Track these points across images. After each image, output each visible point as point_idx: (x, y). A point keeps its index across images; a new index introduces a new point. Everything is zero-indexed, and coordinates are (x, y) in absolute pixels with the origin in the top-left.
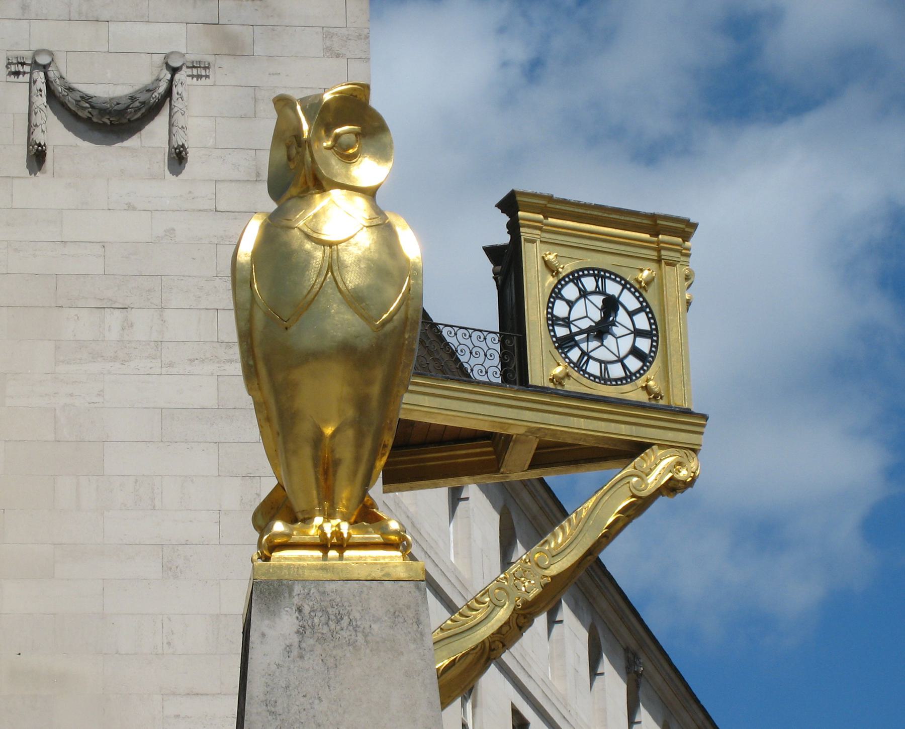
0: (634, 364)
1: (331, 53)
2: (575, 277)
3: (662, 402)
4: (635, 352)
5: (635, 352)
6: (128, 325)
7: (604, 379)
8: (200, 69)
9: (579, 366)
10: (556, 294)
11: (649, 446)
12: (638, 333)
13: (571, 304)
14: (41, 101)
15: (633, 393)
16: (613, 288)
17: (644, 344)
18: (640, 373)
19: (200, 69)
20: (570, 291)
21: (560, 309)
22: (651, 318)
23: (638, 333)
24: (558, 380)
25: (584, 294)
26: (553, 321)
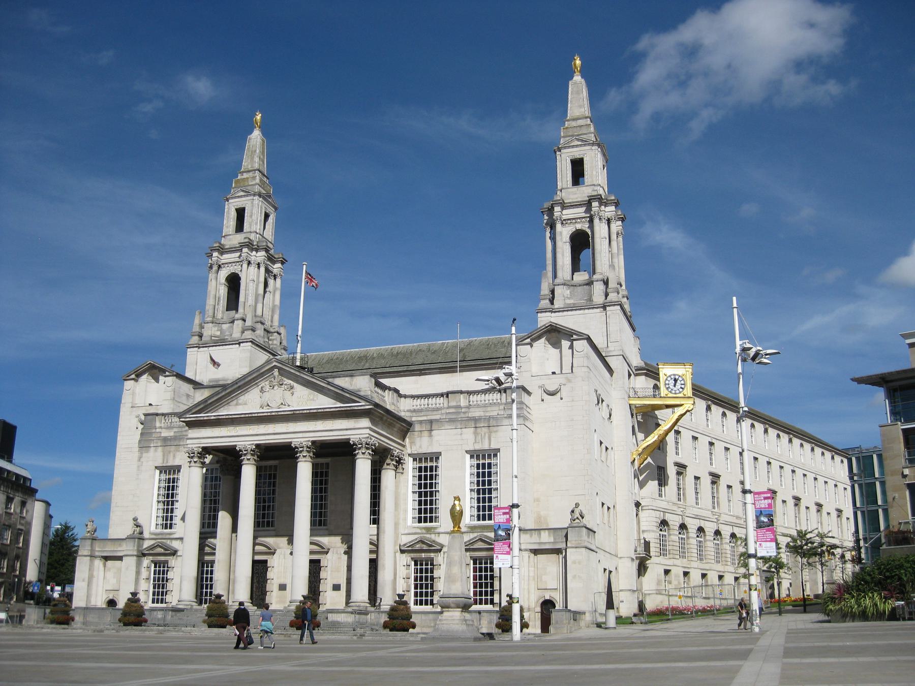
0: (681, 390)
1: (583, 381)
2: (670, 376)
3: (686, 396)
4: (681, 388)
5: (681, 388)
6: (555, 425)
7: (675, 394)
8: (564, 385)
9: (670, 392)
10: (666, 380)
11: (683, 404)
12: (682, 384)
13: (669, 381)
14: (543, 392)
15: (681, 395)
16: (677, 377)
17: (683, 386)
18: (682, 391)
19: (564, 385)
20: (669, 379)
21: (667, 382)
22: (684, 382)
23: (682, 384)
24: (666, 395)
25: (672, 379)
26: (666, 384)
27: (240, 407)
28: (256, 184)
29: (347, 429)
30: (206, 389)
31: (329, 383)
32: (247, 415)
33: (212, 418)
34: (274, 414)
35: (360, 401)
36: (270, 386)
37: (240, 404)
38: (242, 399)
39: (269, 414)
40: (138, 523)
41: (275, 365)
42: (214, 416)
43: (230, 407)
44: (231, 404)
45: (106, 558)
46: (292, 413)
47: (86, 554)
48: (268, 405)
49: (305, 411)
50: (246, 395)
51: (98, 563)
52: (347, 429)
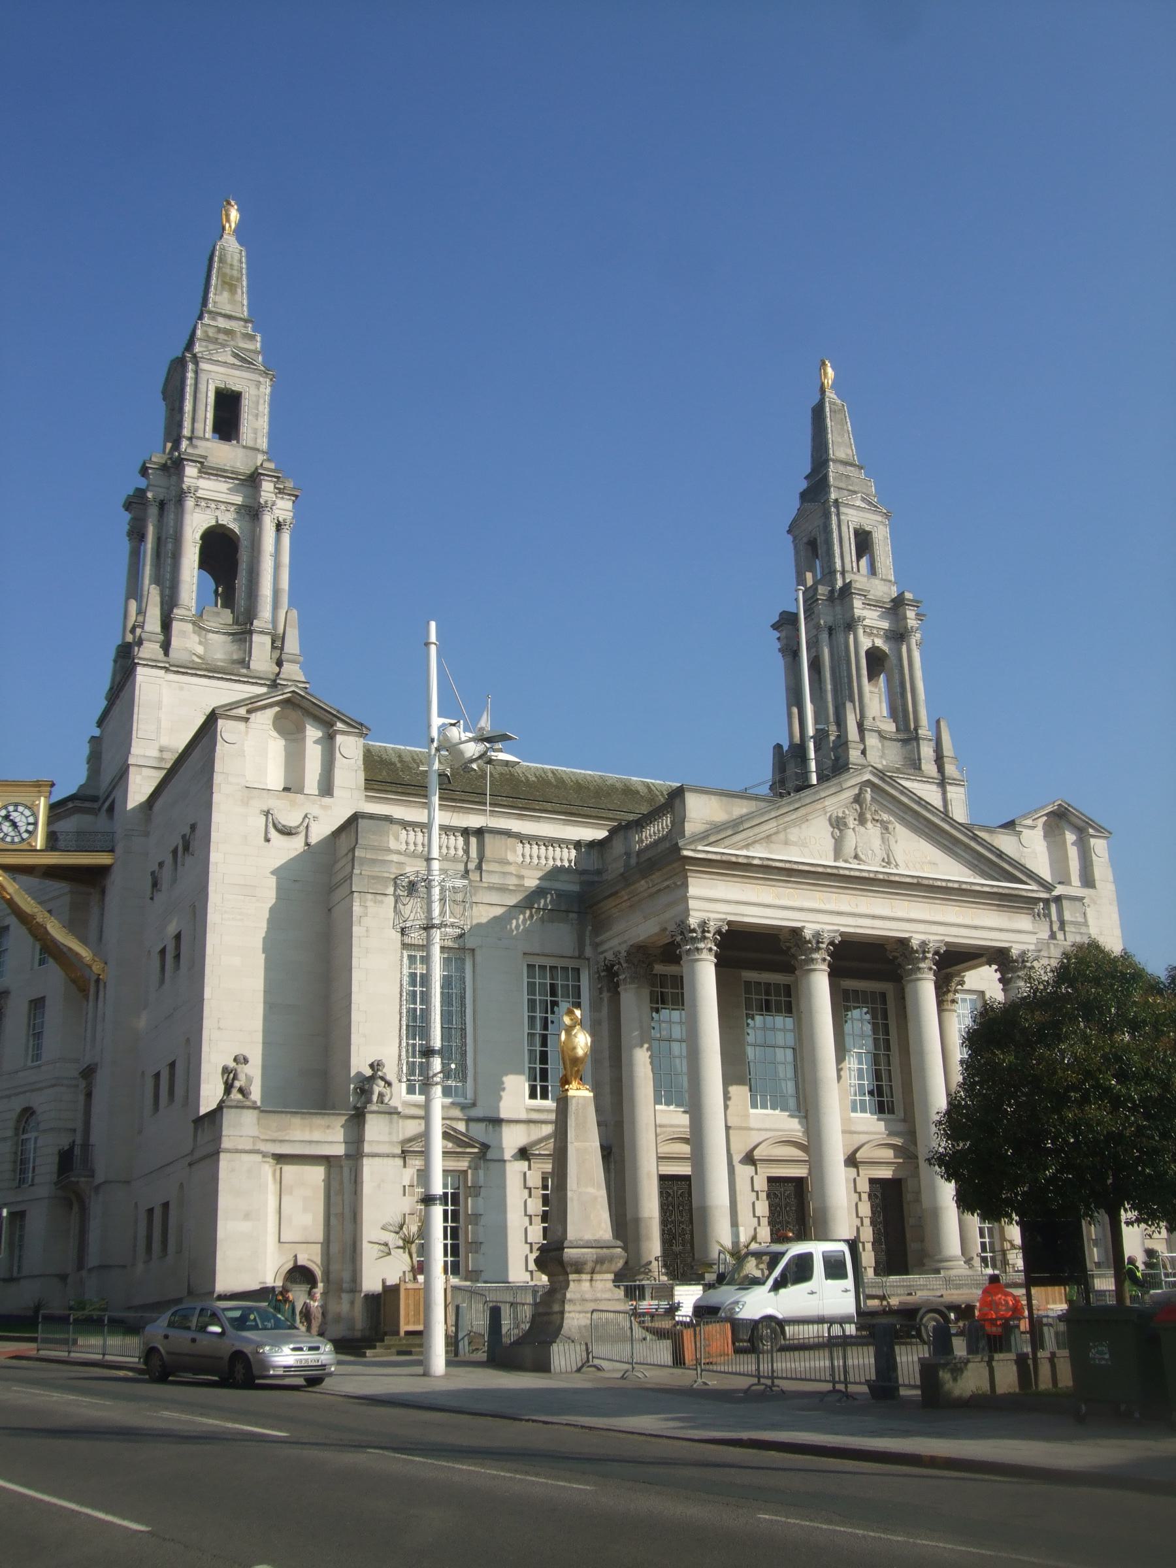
27: (794, 849)
28: (255, 352)
29: (1001, 930)
30: (713, 797)
31: (975, 838)
32: (829, 871)
33: (756, 862)
34: (881, 877)
35: (1029, 881)
36: (855, 819)
37: (795, 844)
38: (794, 834)
39: (872, 875)
40: (385, 1074)
41: (868, 781)
42: (760, 858)
43: (772, 845)
44: (774, 838)
45: (280, 1158)
46: (915, 881)
47: (249, 1147)
48: (856, 857)
49: (939, 883)
50: (804, 826)
51: (268, 1169)
52: (1001, 930)
